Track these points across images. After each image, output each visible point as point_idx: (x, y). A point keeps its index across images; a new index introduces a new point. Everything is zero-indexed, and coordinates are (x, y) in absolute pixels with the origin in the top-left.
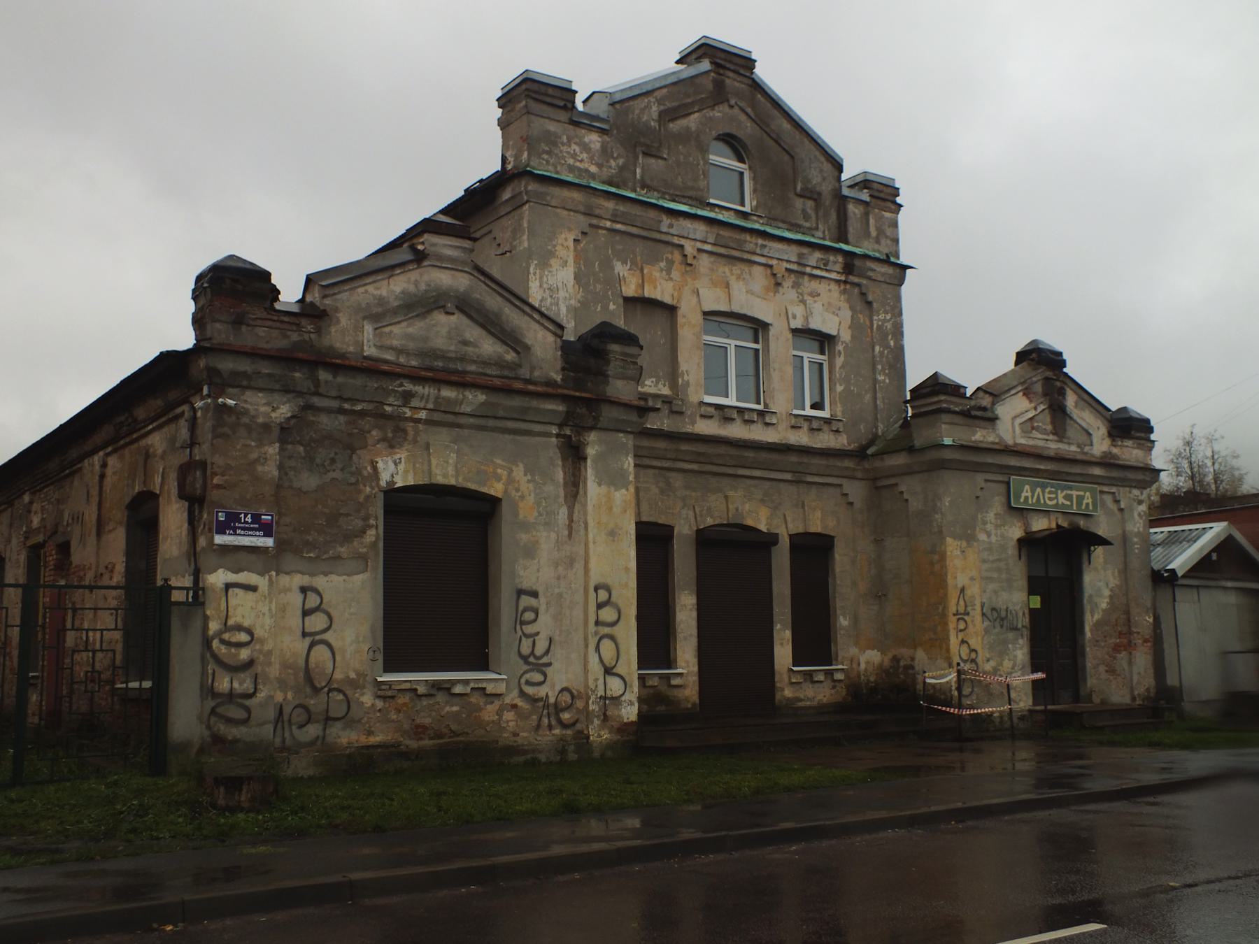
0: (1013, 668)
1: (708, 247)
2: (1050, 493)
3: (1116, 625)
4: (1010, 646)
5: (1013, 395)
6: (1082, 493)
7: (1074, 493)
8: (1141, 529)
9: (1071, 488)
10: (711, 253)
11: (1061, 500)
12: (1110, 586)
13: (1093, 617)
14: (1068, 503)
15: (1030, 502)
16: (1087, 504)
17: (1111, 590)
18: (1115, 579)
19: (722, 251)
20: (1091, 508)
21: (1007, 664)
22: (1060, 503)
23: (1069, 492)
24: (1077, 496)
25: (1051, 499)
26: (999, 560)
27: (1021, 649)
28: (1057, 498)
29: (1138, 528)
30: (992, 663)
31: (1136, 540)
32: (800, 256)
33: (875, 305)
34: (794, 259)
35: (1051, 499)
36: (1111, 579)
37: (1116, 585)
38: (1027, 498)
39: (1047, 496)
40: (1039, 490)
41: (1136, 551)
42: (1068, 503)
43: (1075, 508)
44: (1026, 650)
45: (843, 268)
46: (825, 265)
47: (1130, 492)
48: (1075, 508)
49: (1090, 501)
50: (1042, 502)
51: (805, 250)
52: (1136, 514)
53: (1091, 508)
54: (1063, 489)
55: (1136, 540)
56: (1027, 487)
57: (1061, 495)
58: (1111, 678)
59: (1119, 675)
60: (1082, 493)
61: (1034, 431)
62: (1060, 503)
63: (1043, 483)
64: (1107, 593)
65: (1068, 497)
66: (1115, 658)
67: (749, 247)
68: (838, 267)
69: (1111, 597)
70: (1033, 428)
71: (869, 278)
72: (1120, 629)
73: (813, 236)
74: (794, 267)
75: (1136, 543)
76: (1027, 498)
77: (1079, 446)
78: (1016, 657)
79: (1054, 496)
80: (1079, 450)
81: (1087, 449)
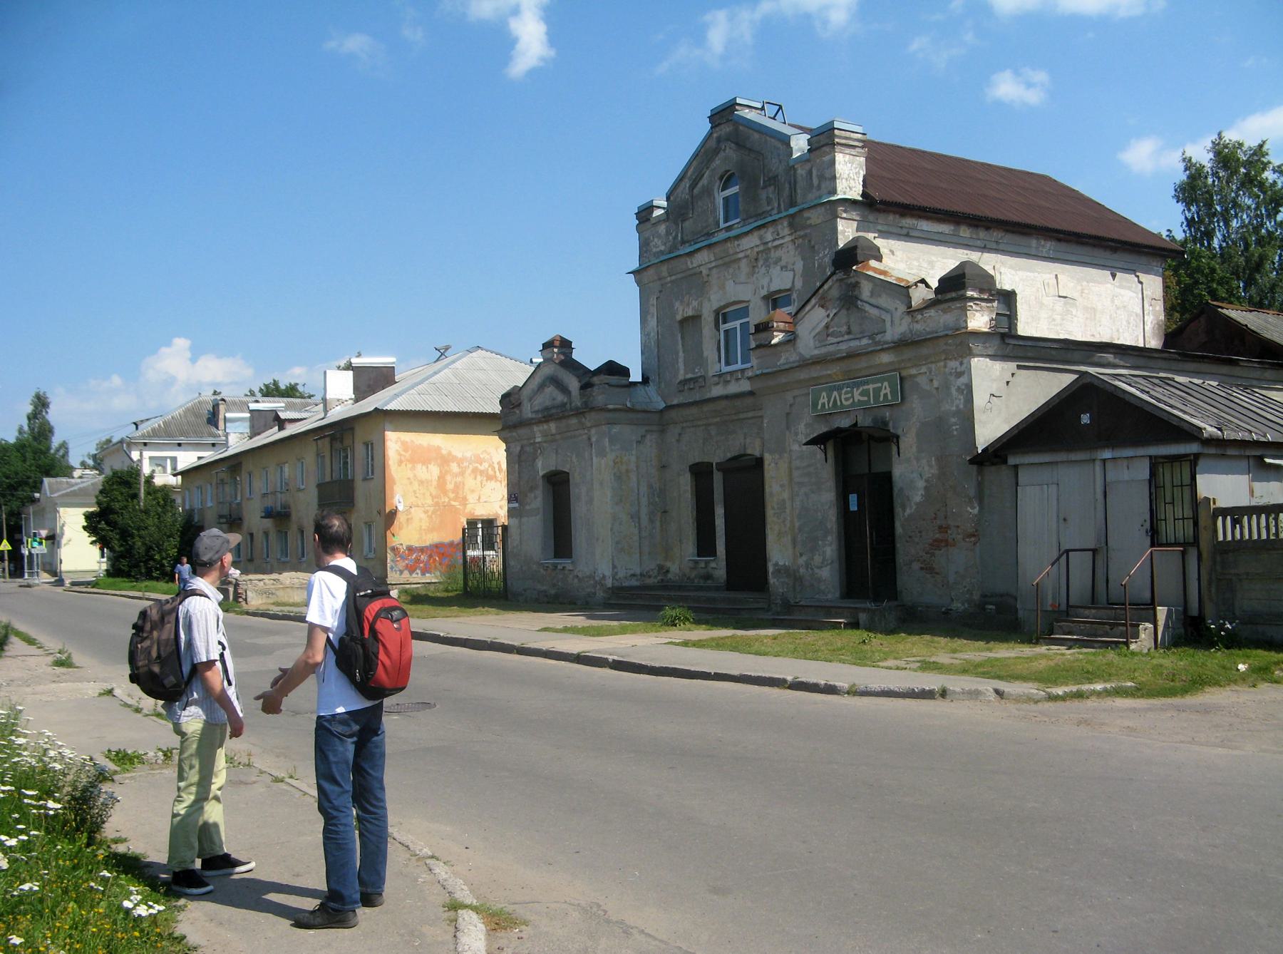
0: (822, 563)
1: (713, 264)
2: (846, 393)
3: (935, 518)
4: (820, 542)
5: (809, 311)
6: (880, 385)
7: (871, 387)
8: (961, 406)
9: (867, 383)
10: (715, 267)
11: (857, 397)
12: (927, 475)
13: (904, 510)
14: (866, 399)
15: (827, 407)
16: (885, 395)
17: (927, 481)
18: (930, 466)
19: (720, 262)
20: (890, 398)
21: (817, 559)
22: (856, 400)
23: (865, 387)
24: (874, 389)
25: (847, 399)
26: (809, 466)
27: (830, 545)
28: (853, 397)
29: (957, 406)
30: (804, 558)
31: (953, 420)
32: (761, 238)
33: (816, 247)
34: (758, 242)
35: (847, 399)
36: (926, 468)
37: (933, 474)
38: (823, 405)
39: (843, 397)
40: (835, 393)
41: (955, 433)
42: (866, 399)
43: (872, 402)
44: (834, 546)
45: (791, 229)
46: (778, 235)
47: (945, 366)
48: (872, 402)
49: (888, 390)
50: (839, 403)
51: (762, 232)
52: (953, 391)
53: (890, 398)
54: (858, 385)
55: (953, 420)
56: (824, 394)
57: (856, 393)
58: (928, 576)
59: (937, 573)
60: (880, 385)
61: (829, 338)
62: (856, 400)
63: (839, 386)
64: (921, 484)
65: (863, 393)
66: (933, 555)
67: (731, 251)
68: (786, 231)
69: (926, 488)
70: (828, 336)
71: (810, 225)
72: (938, 523)
73: (771, 215)
74: (761, 248)
75: (955, 424)
76: (823, 405)
77: (871, 337)
78: (824, 552)
79: (850, 395)
80: (870, 341)
81: (878, 338)
